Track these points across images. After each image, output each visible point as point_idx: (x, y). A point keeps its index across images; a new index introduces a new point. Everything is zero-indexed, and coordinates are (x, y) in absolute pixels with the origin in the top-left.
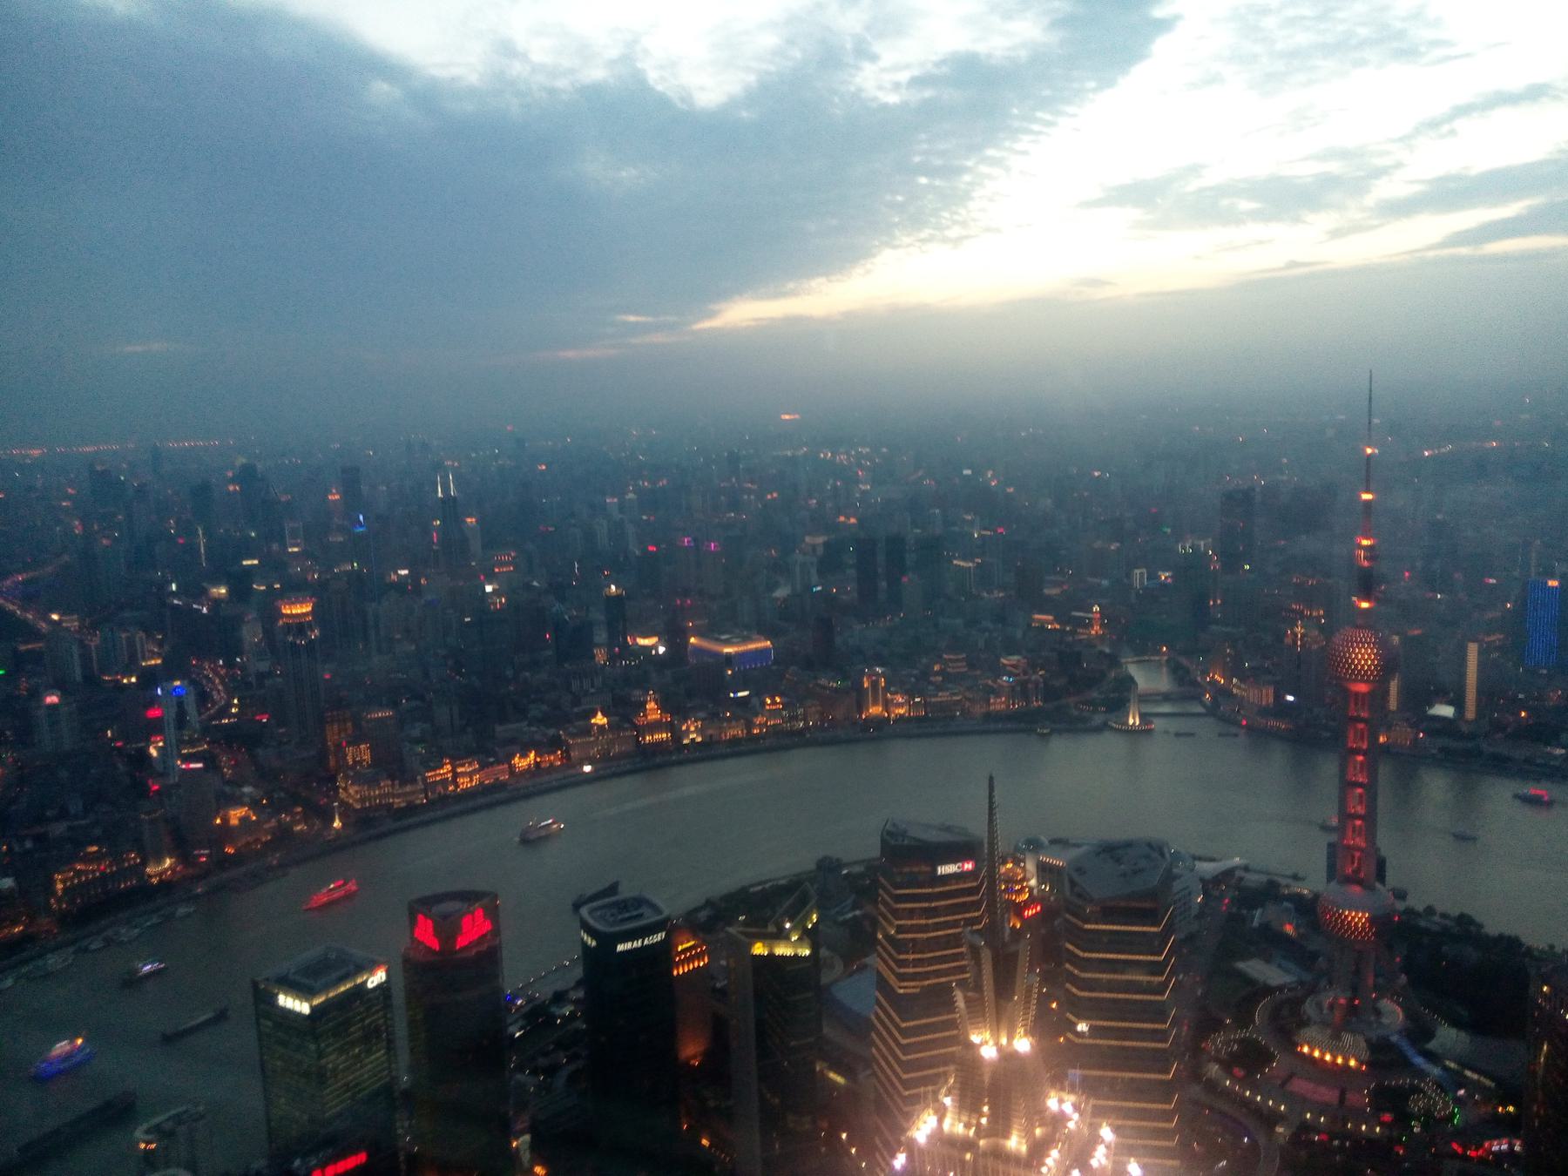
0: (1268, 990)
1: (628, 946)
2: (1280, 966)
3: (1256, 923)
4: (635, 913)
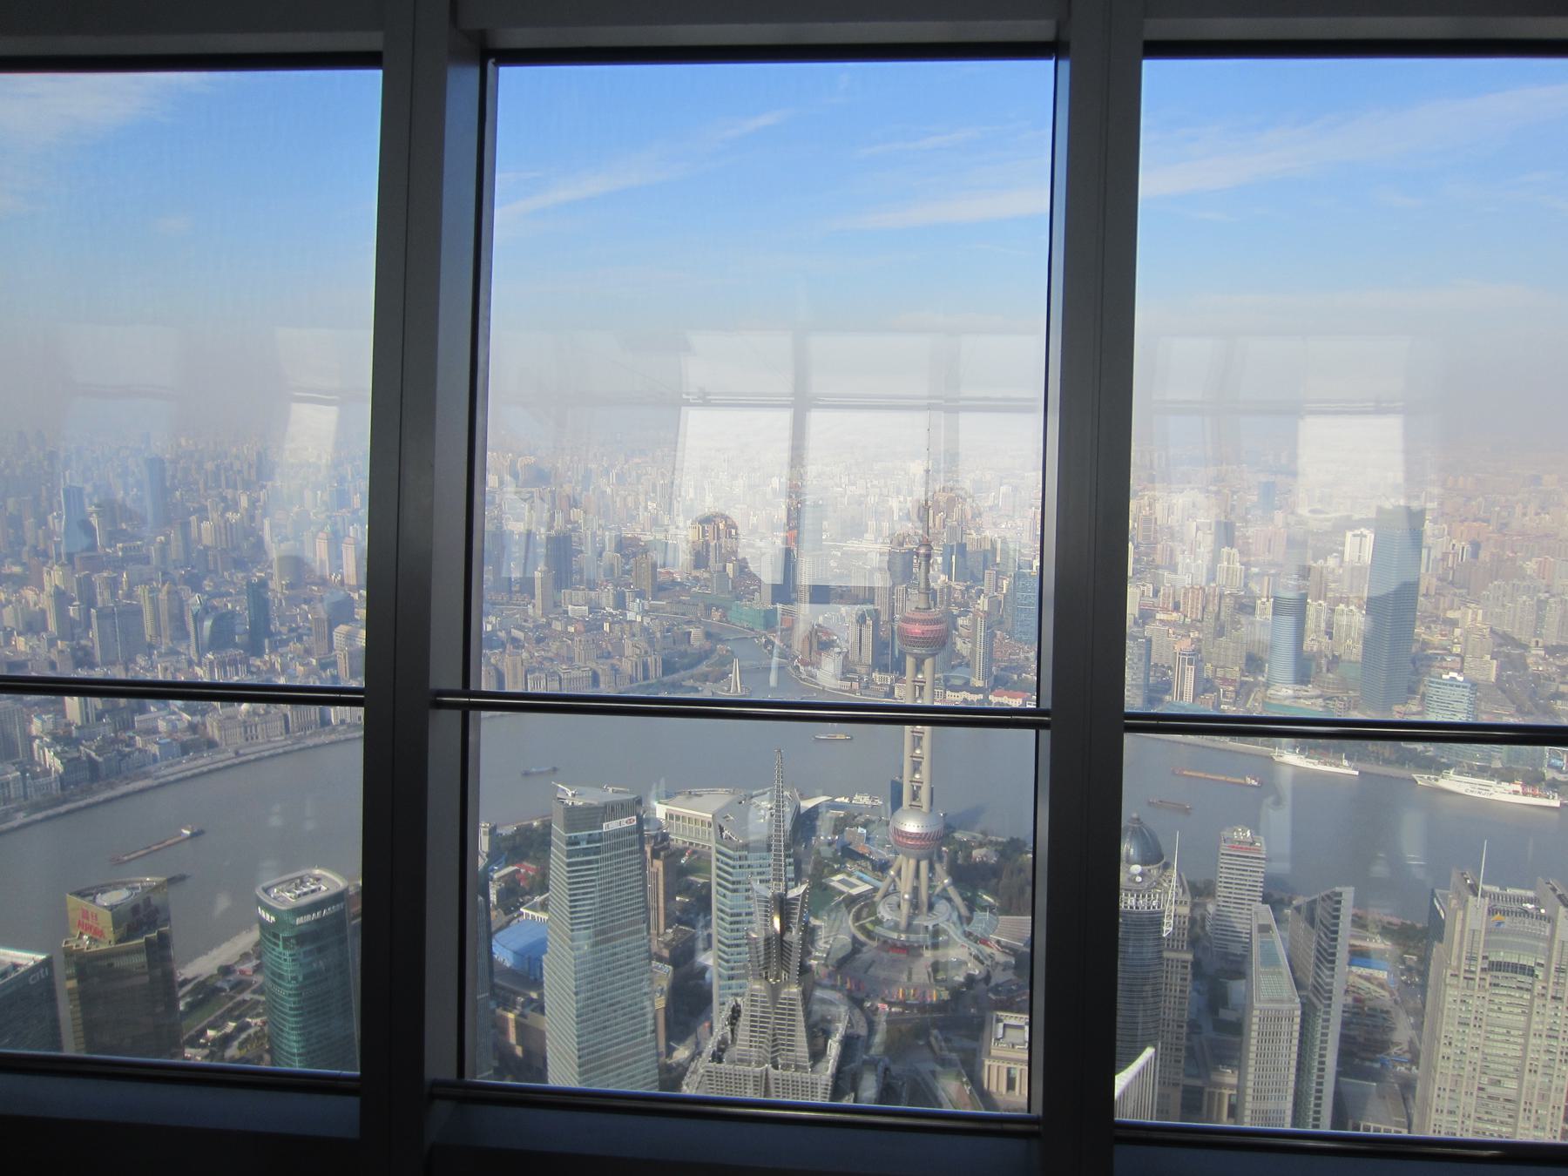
2: (860, 879)
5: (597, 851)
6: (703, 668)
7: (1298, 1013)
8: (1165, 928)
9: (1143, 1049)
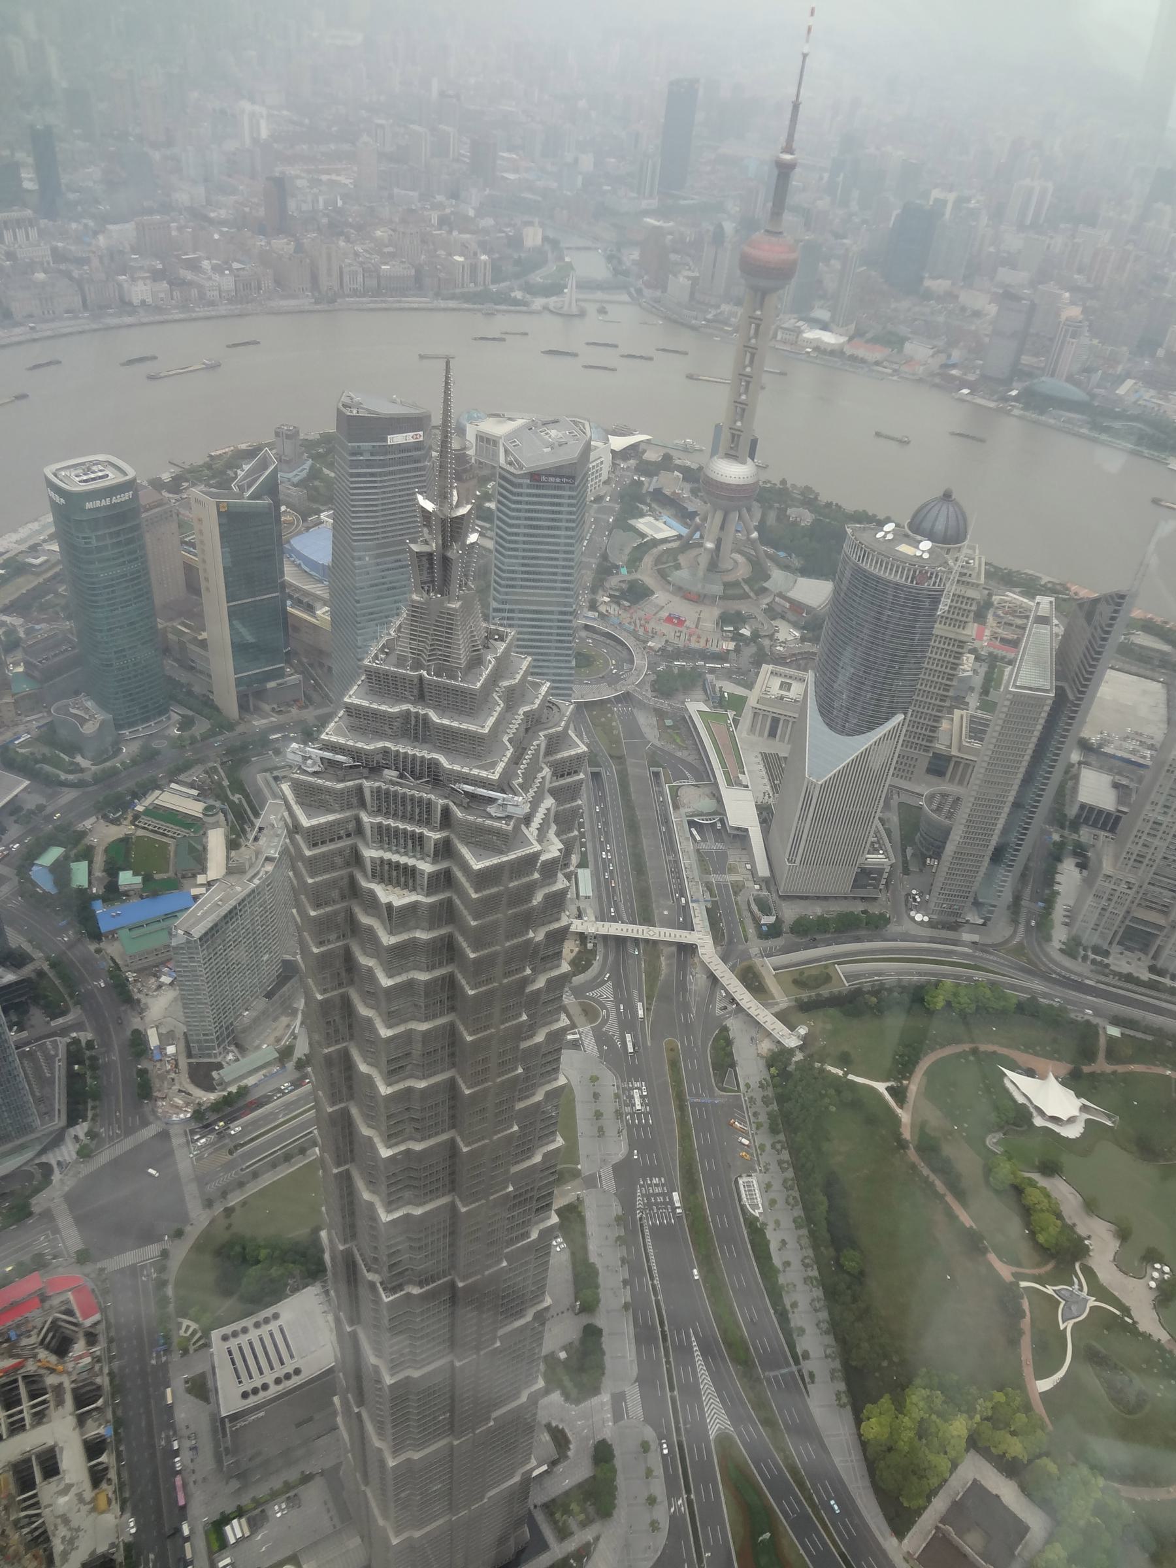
0: (655, 543)
1: (98, 504)
2: (665, 523)
3: (651, 490)
4: (100, 474)
5: (383, 464)
6: (537, 278)
7: (1050, 702)
8: (940, 607)
9: (894, 714)
